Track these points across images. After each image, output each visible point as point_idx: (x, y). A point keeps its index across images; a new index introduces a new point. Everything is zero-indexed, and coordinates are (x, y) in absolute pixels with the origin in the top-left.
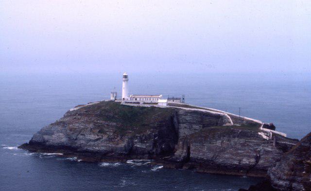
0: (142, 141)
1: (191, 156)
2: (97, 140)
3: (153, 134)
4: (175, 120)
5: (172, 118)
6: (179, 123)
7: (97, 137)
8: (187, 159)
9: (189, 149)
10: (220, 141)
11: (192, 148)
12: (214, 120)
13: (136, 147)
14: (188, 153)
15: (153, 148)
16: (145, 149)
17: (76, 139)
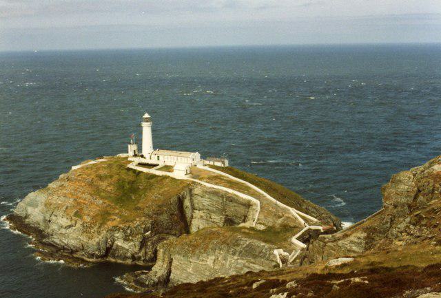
0: (126, 239)
1: (172, 276)
2: (70, 227)
3: (143, 226)
4: (187, 203)
5: (181, 202)
6: (193, 208)
7: (69, 223)
8: (166, 280)
9: (171, 263)
10: (213, 258)
11: (175, 263)
12: (242, 210)
13: (117, 246)
14: (169, 272)
15: (141, 249)
16: (127, 250)
17: (50, 221)
